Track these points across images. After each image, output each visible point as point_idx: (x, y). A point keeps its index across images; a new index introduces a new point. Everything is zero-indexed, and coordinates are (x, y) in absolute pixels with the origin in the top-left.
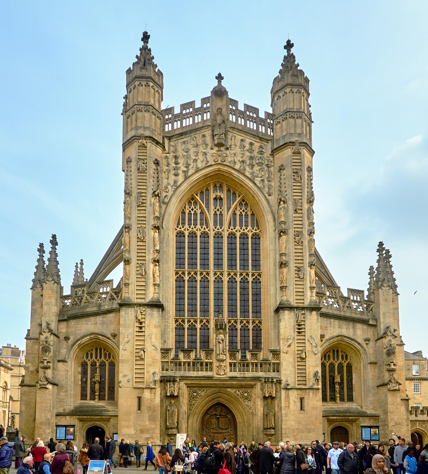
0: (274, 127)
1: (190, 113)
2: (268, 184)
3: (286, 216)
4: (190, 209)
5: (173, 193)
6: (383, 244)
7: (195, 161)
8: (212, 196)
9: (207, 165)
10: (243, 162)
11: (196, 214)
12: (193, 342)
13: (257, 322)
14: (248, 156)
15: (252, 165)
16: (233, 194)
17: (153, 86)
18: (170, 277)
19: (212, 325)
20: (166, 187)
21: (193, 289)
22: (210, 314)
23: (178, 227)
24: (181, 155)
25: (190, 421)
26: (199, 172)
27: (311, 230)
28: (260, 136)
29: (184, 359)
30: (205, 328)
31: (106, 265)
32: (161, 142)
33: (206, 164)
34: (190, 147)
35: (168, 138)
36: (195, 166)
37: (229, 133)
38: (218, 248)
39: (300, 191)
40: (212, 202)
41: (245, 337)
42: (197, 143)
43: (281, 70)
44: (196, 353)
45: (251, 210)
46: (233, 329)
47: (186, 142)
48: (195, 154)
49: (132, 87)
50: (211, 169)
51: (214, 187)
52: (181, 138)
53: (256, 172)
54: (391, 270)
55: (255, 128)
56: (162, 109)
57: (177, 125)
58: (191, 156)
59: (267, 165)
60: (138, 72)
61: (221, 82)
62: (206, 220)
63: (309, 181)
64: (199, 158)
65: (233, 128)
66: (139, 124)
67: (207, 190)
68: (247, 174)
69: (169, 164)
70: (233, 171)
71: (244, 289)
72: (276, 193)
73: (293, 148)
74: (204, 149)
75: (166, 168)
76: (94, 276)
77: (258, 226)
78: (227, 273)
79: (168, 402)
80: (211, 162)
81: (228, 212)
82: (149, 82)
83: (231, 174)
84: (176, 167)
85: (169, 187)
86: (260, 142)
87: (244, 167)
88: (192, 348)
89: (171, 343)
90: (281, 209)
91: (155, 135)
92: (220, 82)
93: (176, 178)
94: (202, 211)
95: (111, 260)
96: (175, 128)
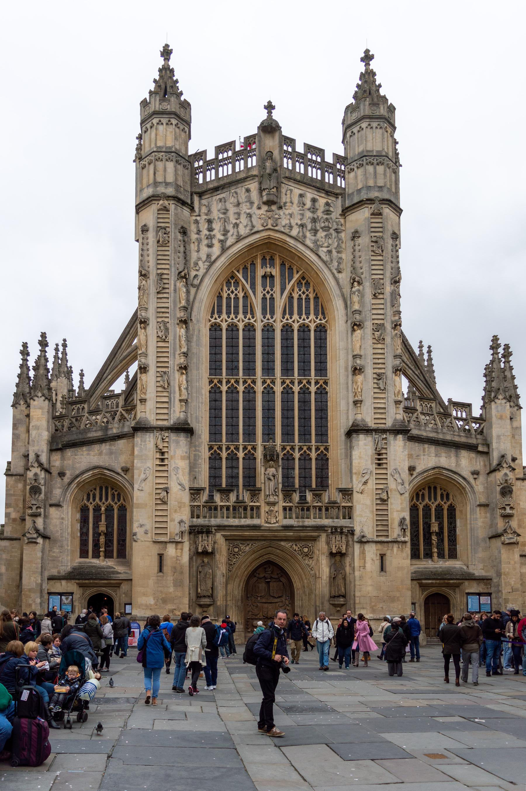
0: (346, 176)
1: (228, 158)
2: (337, 256)
3: (361, 302)
4: (229, 292)
5: (205, 271)
6: (498, 339)
7: (236, 225)
8: (260, 272)
9: (253, 231)
10: (302, 226)
11: (238, 298)
12: (233, 477)
13: (322, 448)
14: (309, 218)
15: (315, 230)
16: (288, 269)
17: (177, 124)
18: (202, 388)
19: (259, 454)
20: (196, 264)
21: (233, 409)
22: (257, 439)
23: (212, 317)
24: (216, 218)
25: (230, 587)
26: (241, 242)
27: (396, 321)
28: (326, 188)
29: (222, 501)
30: (250, 458)
31: (111, 370)
32: (189, 202)
33: (251, 230)
34: (229, 206)
35: (198, 195)
36: (235, 233)
37: (283, 185)
38: (268, 346)
39: (381, 267)
40: (259, 281)
41: (305, 469)
42: (238, 201)
43: (356, 92)
44: (238, 492)
45: (314, 291)
46: (289, 458)
47: (223, 200)
48: (236, 216)
49: (148, 126)
50: (257, 236)
51: (262, 259)
52: (216, 193)
53: (320, 239)
54: (511, 373)
55: (319, 178)
56: (190, 154)
57: (211, 175)
58: (231, 219)
59: (336, 229)
60: (156, 105)
61: (272, 113)
62: (251, 307)
63: (394, 252)
64: (240, 222)
65: (289, 178)
66: (160, 179)
67: (253, 264)
68: (308, 242)
69: (200, 231)
70: (288, 239)
71: (304, 403)
72: (349, 269)
73: (371, 208)
74: (248, 209)
75: (196, 236)
76: (96, 385)
77: (323, 313)
78: (281, 381)
79: (199, 561)
80: (259, 227)
81: (282, 294)
82: (171, 120)
83: (285, 242)
84: (210, 235)
85: (200, 263)
86: (325, 197)
87: (303, 233)
88: (232, 486)
89: (204, 481)
90: (354, 293)
91: (180, 193)
92: (270, 113)
93: (210, 250)
94: (245, 293)
95: (118, 361)
96: (208, 179)
